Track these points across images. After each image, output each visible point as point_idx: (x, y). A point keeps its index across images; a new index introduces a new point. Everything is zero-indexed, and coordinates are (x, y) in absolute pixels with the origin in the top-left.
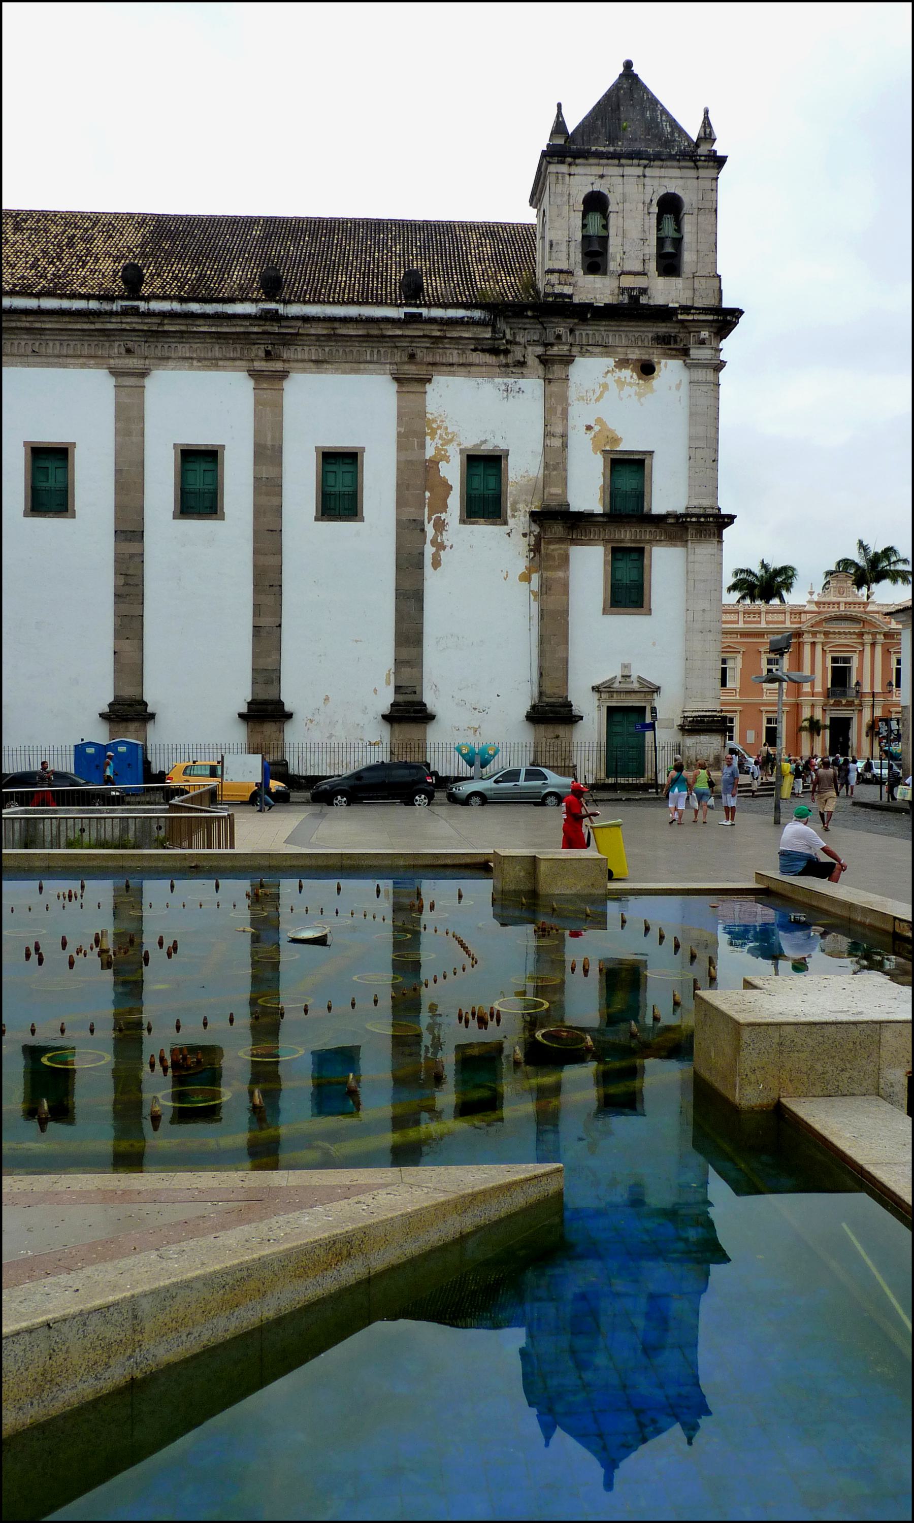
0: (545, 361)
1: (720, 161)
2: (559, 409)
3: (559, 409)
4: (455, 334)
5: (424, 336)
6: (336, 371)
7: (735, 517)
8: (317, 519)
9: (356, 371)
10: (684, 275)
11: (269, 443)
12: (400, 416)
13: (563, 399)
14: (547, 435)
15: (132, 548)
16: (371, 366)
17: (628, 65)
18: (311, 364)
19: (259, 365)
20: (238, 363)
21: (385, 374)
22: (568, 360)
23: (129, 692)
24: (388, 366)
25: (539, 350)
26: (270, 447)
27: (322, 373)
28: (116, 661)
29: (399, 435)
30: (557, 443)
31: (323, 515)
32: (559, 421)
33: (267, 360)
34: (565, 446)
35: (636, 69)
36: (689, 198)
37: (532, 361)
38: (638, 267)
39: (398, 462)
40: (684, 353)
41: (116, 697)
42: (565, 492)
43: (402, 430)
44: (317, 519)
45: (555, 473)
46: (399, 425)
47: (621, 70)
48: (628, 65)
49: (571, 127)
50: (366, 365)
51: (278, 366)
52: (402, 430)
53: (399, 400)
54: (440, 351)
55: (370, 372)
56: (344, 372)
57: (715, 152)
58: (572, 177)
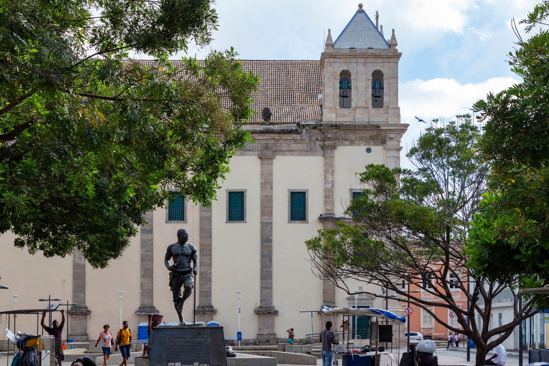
0: (323, 148)
1: (398, 56)
2: (330, 170)
3: (330, 170)
4: (285, 138)
5: (272, 139)
7: (408, 125)
8: (227, 222)
9: (243, 155)
10: (384, 107)
12: (262, 174)
13: (332, 165)
14: (326, 182)
15: (148, 236)
16: (249, 152)
17: (361, 6)
23: (147, 302)
24: (256, 152)
25: (321, 143)
28: (142, 288)
29: (262, 183)
30: (329, 186)
32: (330, 177)
34: (333, 186)
35: (364, 8)
36: (385, 71)
37: (318, 148)
38: (364, 104)
39: (261, 196)
40: (383, 142)
41: (141, 304)
42: (333, 209)
43: (263, 181)
44: (227, 222)
45: (328, 200)
46: (262, 179)
47: (357, 8)
48: (361, 6)
49: (334, 39)
50: (247, 152)
52: (263, 181)
53: (261, 167)
54: (279, 145)
55: (250, 155)
57: (397, 50)
58: (335, 64)
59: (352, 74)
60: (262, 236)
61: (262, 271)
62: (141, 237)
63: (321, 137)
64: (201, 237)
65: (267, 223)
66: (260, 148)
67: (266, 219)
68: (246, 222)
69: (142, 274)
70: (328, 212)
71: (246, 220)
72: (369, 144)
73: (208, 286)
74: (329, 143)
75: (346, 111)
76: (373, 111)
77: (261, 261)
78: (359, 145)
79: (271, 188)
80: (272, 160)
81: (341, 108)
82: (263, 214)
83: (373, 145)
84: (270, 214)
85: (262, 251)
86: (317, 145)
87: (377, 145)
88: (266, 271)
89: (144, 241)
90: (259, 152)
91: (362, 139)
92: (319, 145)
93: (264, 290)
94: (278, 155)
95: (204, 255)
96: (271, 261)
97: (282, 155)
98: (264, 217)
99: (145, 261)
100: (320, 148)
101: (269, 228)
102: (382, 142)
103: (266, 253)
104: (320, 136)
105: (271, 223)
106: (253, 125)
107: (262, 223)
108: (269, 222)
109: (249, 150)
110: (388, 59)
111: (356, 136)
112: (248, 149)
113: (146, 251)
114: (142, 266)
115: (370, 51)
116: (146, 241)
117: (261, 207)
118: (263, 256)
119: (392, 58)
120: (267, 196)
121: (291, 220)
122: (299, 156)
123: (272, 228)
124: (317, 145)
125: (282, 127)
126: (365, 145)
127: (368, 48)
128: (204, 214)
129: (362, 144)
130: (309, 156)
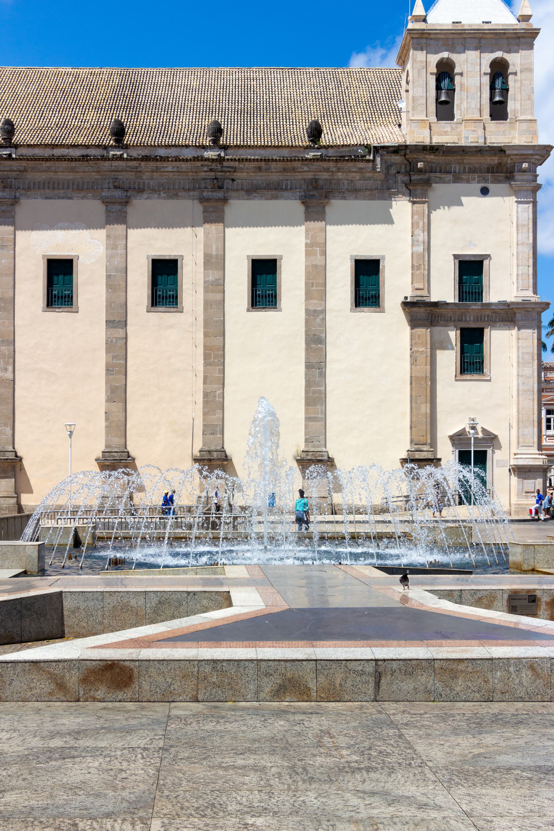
6: (261, 197)
8: (248, 310)
9: (276, 198)
11: (214, 253)
18: (243, 193)
19: (205, 194)
20: (191, 193)
21: (296, 199)
22: (428, 183)
25: (406, 178)
26: (215, 256)
27: (250, 199)
28: (107, 419)
29: (307, 245)
31: (252, 306)
33: (212, 191)
44: (248, 310)
45: (418, 272)
50: (283, 193)
51: (220, 194)
52: (309, 241)
56: (267, 199)
59: (457, 65)
60: (306, 332)
61: (307, 392)
62: (106, 334)
63: (406, 168)
64: (206, 335)
65: (315, 311)
66: (304, 187)
67: (315, 305)
68: (281, 311)
69: (108, 396)
70: (419, 293)
71: (280, 306)
72: (486, 181)
73: (217, 416)
74: (418, 177)
75: (445, 125)
76: (493, 126)
77: (306, 375)
78: (468, 181)
79: (324, 253)
80: (324, 207)
81: (438, 120)
82: (308, 295)
83: (492, 182)
84: (323, 295)
85: (307, 358)
86: (399, 182)
87: (499, 182)
88: (315, 392)
89: (112, 342)
90: (303, 194)
91: (473, 171)
92: (403, 182)
93: (310, 423)
94: (334, 198)
95: (211, 364)
96: (323, 375)
97: (341, 199)
98: (311, 302)
99: (113, 374)
100: (404, 188)
101: (318, 320)
102: (506, 177)
103: (314, 360)
104: (403, 167)
105: (324, 311)
106: (293, 149)
107: (307, 311)
108: (319, 309)
109: (286, 189)
110: (517, 41)
111: (465, 168)
112: (284, 188)
113: (114, 357)
114: (107, 382)
115: (486, 27)
116: (114, 340)
117: (306, 284)
118: (309, 366)
119: (523, 37)
120: (315, 266)
121: (356, 306)
122: (369, 199)
123: (324, 319)
124: (399, 182)
125: (341, 152)
126: (479, 182)
127: (483, 22)
128: (211, 296)
129: (474, 179)
130: (385, 200)
